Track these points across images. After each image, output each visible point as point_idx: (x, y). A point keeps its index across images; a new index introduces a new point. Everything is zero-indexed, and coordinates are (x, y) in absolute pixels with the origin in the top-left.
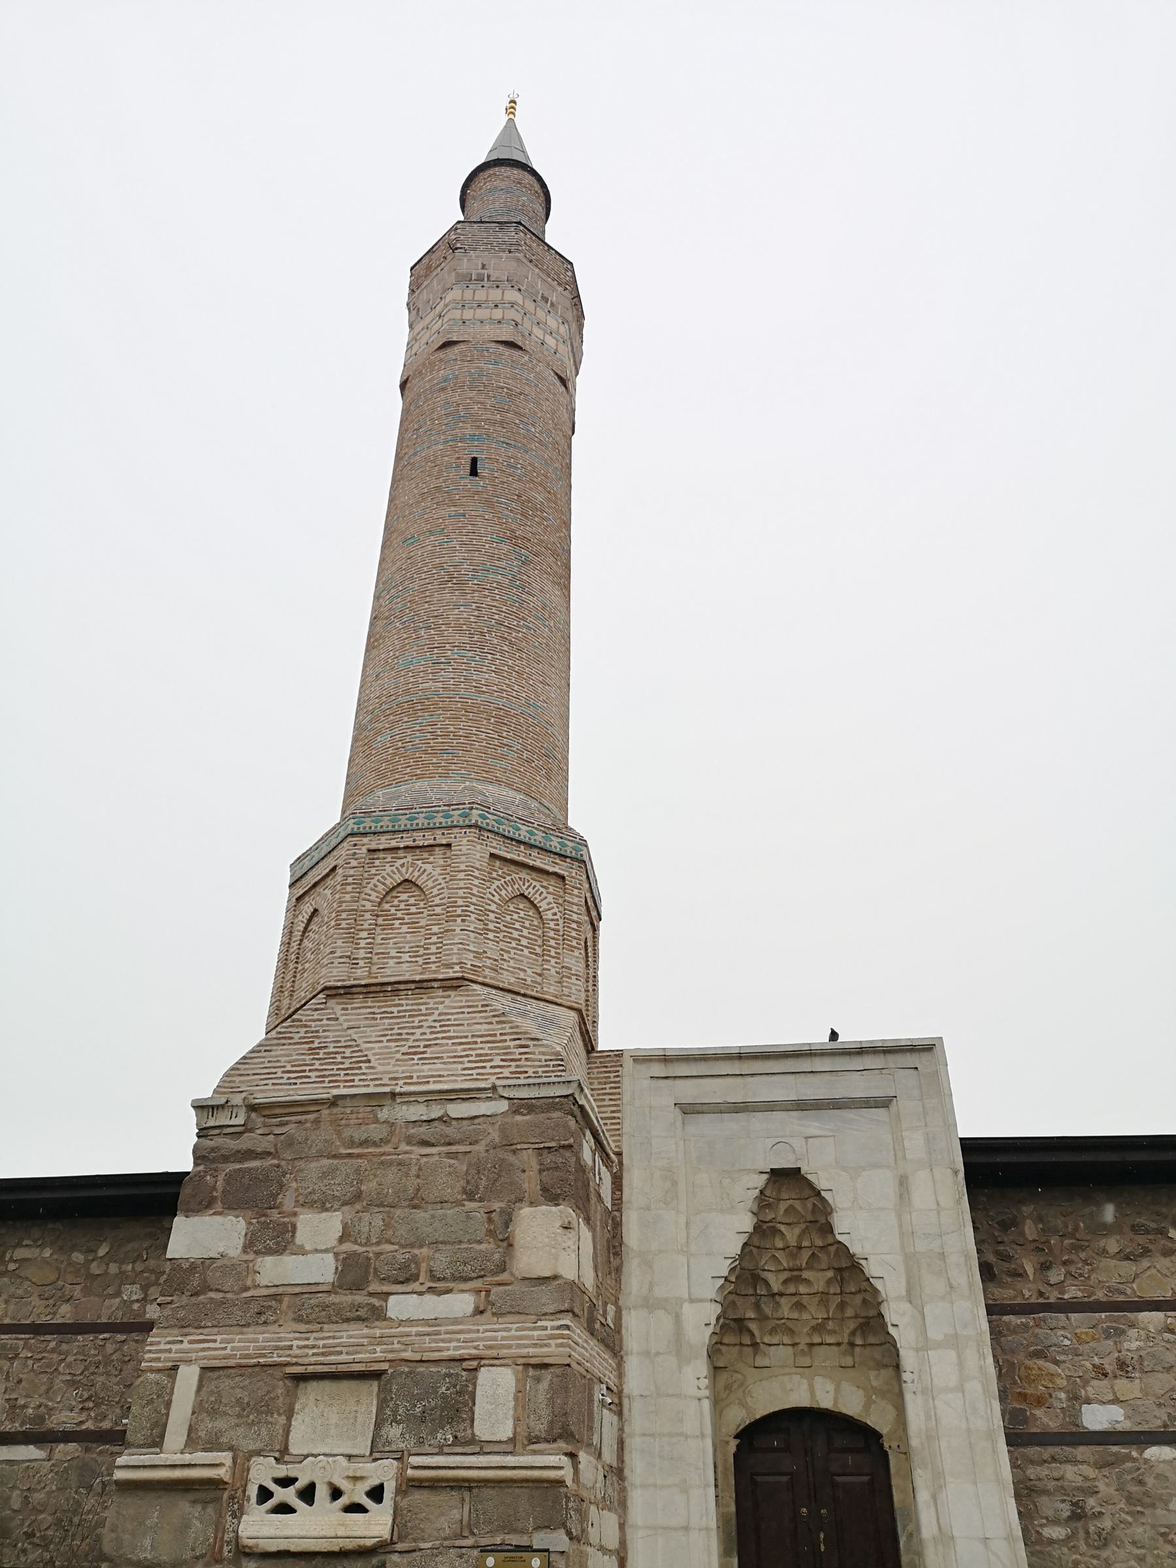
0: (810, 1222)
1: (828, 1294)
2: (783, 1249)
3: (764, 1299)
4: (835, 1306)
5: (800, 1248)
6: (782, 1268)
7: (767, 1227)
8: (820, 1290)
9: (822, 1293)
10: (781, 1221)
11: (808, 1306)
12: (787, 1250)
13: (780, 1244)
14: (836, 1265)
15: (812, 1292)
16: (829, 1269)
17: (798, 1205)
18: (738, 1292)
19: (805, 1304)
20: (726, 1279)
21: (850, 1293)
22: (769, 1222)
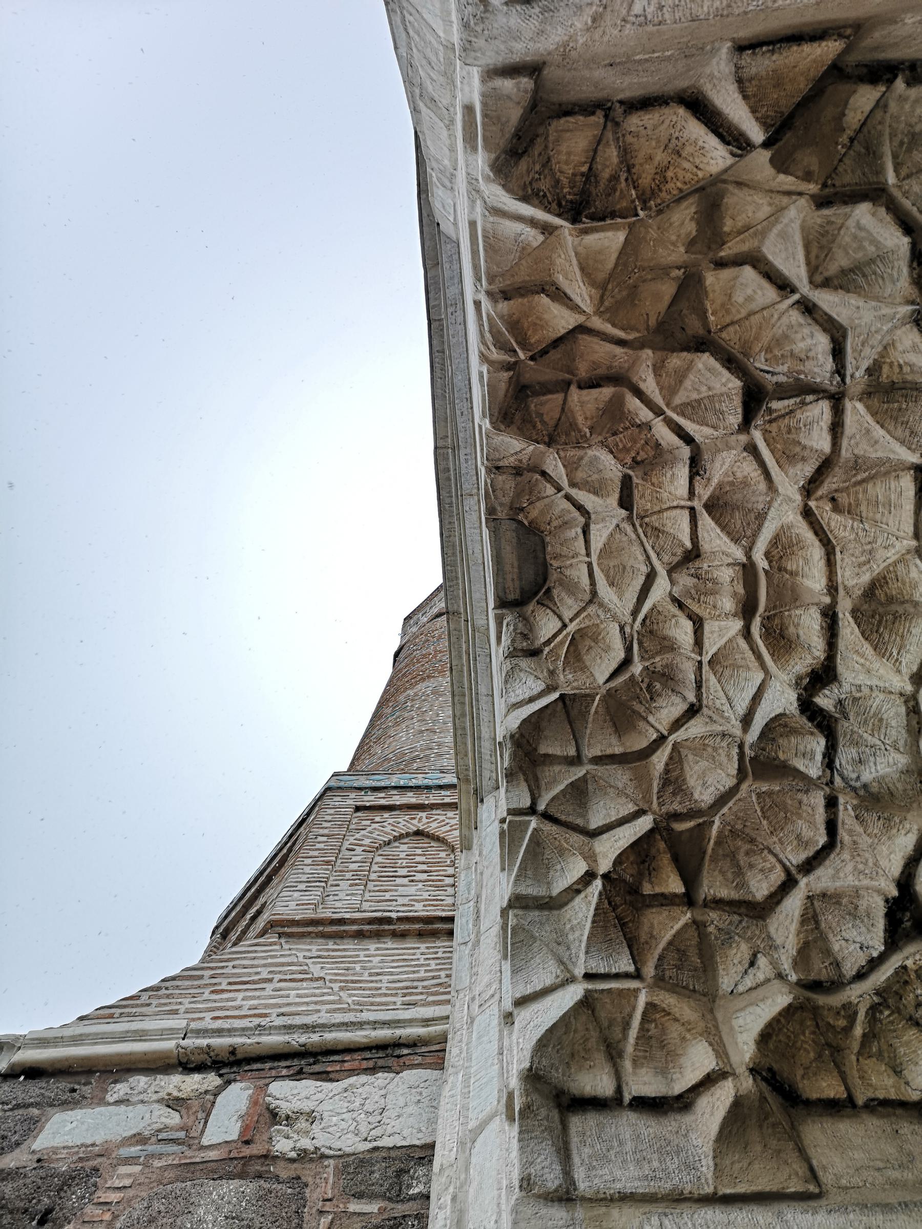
0: (626, 502)
1: (825, 466)
2: (698, 624)
3: (845, 756)
4: (878, 432)
5: (693, 554)
6: (743, 644)
7: (643, 658)
8: (798, 498)
9: (809, 489)
10: (631, 606)
11: (877, 568)
12: (695, 607)
13: (683, 631)
14: (735, 419)
15: (808, 535)
16: (752, 449)
17: (599, 538)
18: (796, 858)
19: (866, 578)
20: (518, 902)
21: (838, 352)
22: (629, 650)
